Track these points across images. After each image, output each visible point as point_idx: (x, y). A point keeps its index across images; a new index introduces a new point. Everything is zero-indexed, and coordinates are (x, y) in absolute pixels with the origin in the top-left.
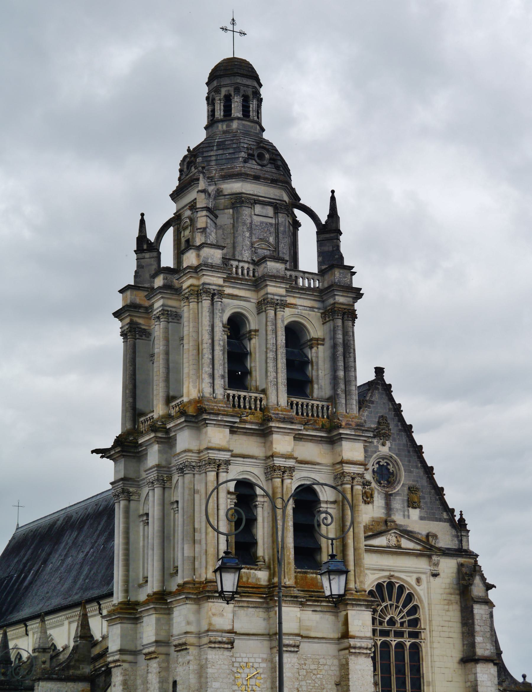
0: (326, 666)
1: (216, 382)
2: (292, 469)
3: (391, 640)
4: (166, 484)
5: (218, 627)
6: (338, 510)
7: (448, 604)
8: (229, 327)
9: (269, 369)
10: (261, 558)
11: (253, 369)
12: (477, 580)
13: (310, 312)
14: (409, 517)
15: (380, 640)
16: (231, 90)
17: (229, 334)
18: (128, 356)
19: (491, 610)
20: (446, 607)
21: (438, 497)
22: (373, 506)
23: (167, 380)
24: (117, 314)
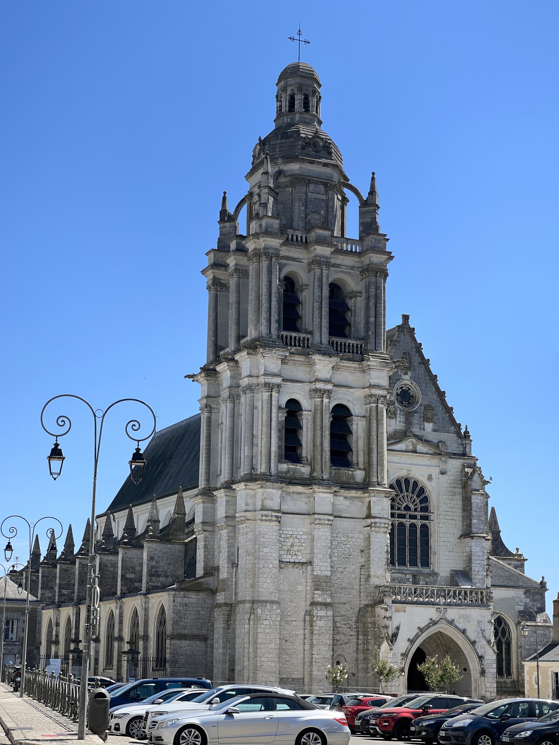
0: (354, 539)
1: (272, 325)
2: (329, 392)
3: (407, 521)
4: (236, 402)
5: (268, 507)
6: (366, 423)
7: (453, 495)
8: (285, 283)
9: (315, 315)
10: (305, 458)
11: (304, 316)
12: (476, 477)
14: (424, 429)
15: (398, 521)
17: (285, 288)
18: (212, 305)
19: (487, 500)
20: (451, 497)
21: (447, 415)
22: (396, 420)
23: (238, 323)
24: (204, 272)
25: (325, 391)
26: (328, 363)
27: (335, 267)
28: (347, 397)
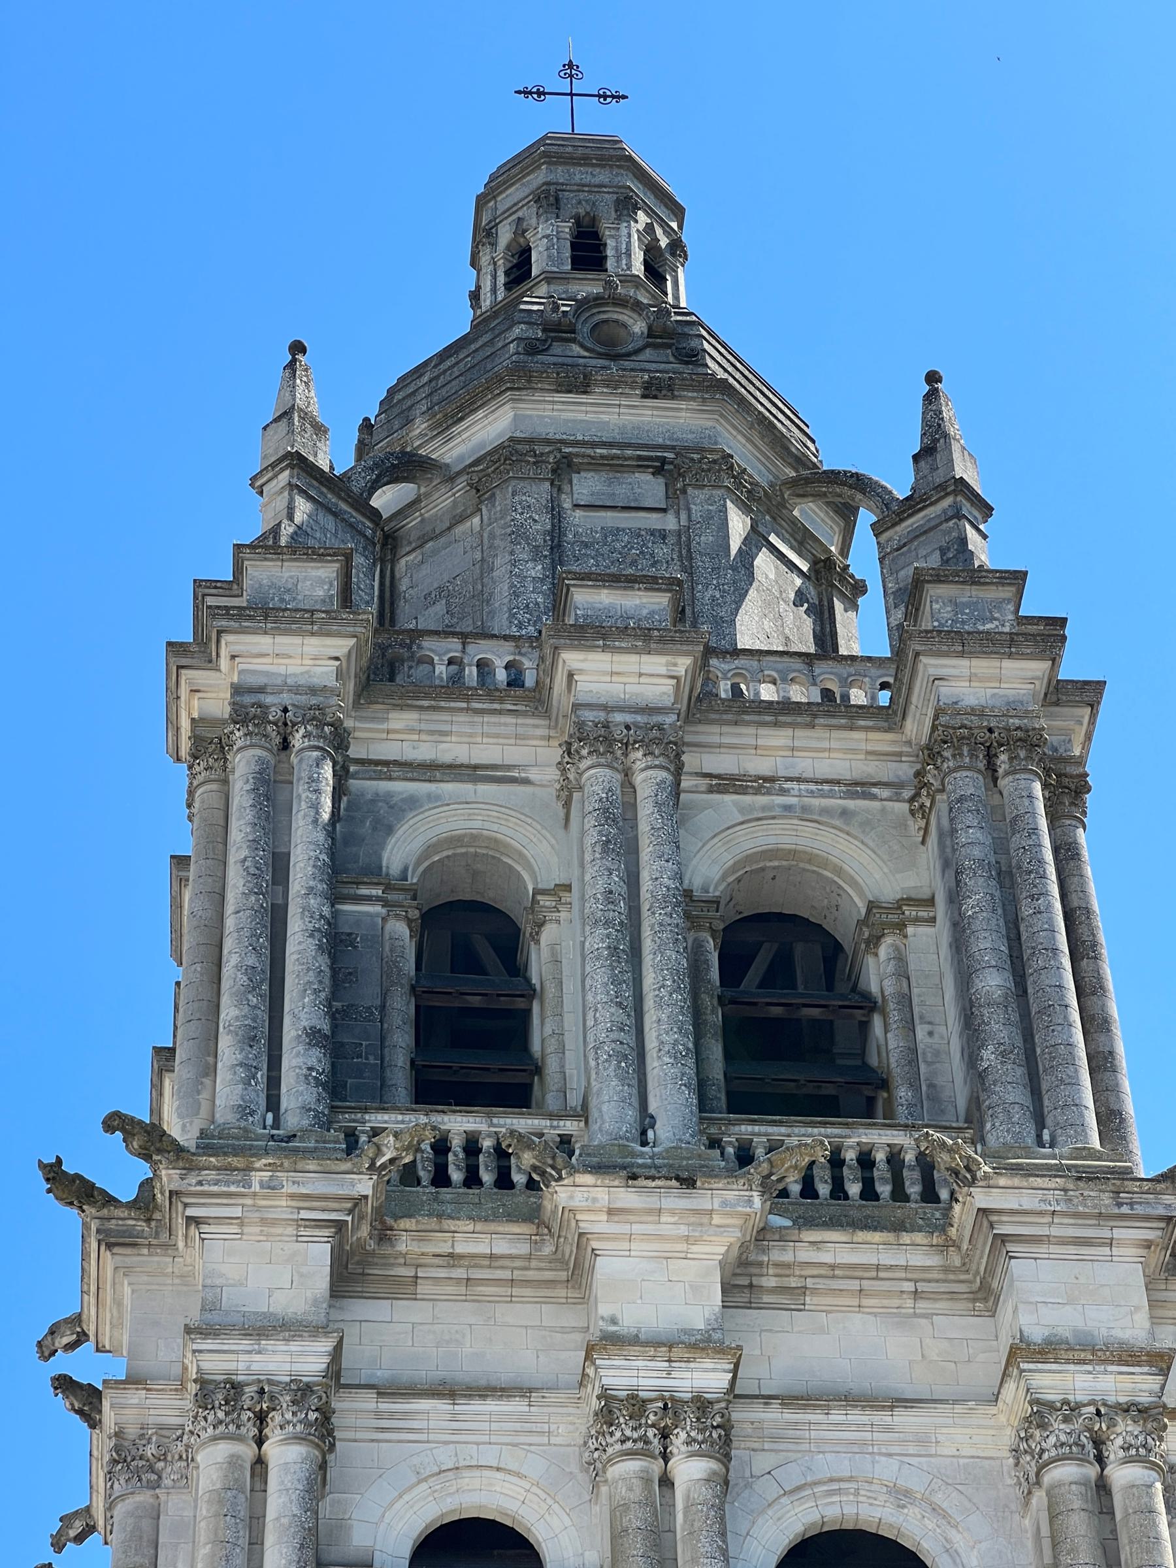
13: (851, 804)
16: (529, 213)
25: (671, 1406)
26: (683, 1230)
27: (743, 791)
28: (887, 1469)
